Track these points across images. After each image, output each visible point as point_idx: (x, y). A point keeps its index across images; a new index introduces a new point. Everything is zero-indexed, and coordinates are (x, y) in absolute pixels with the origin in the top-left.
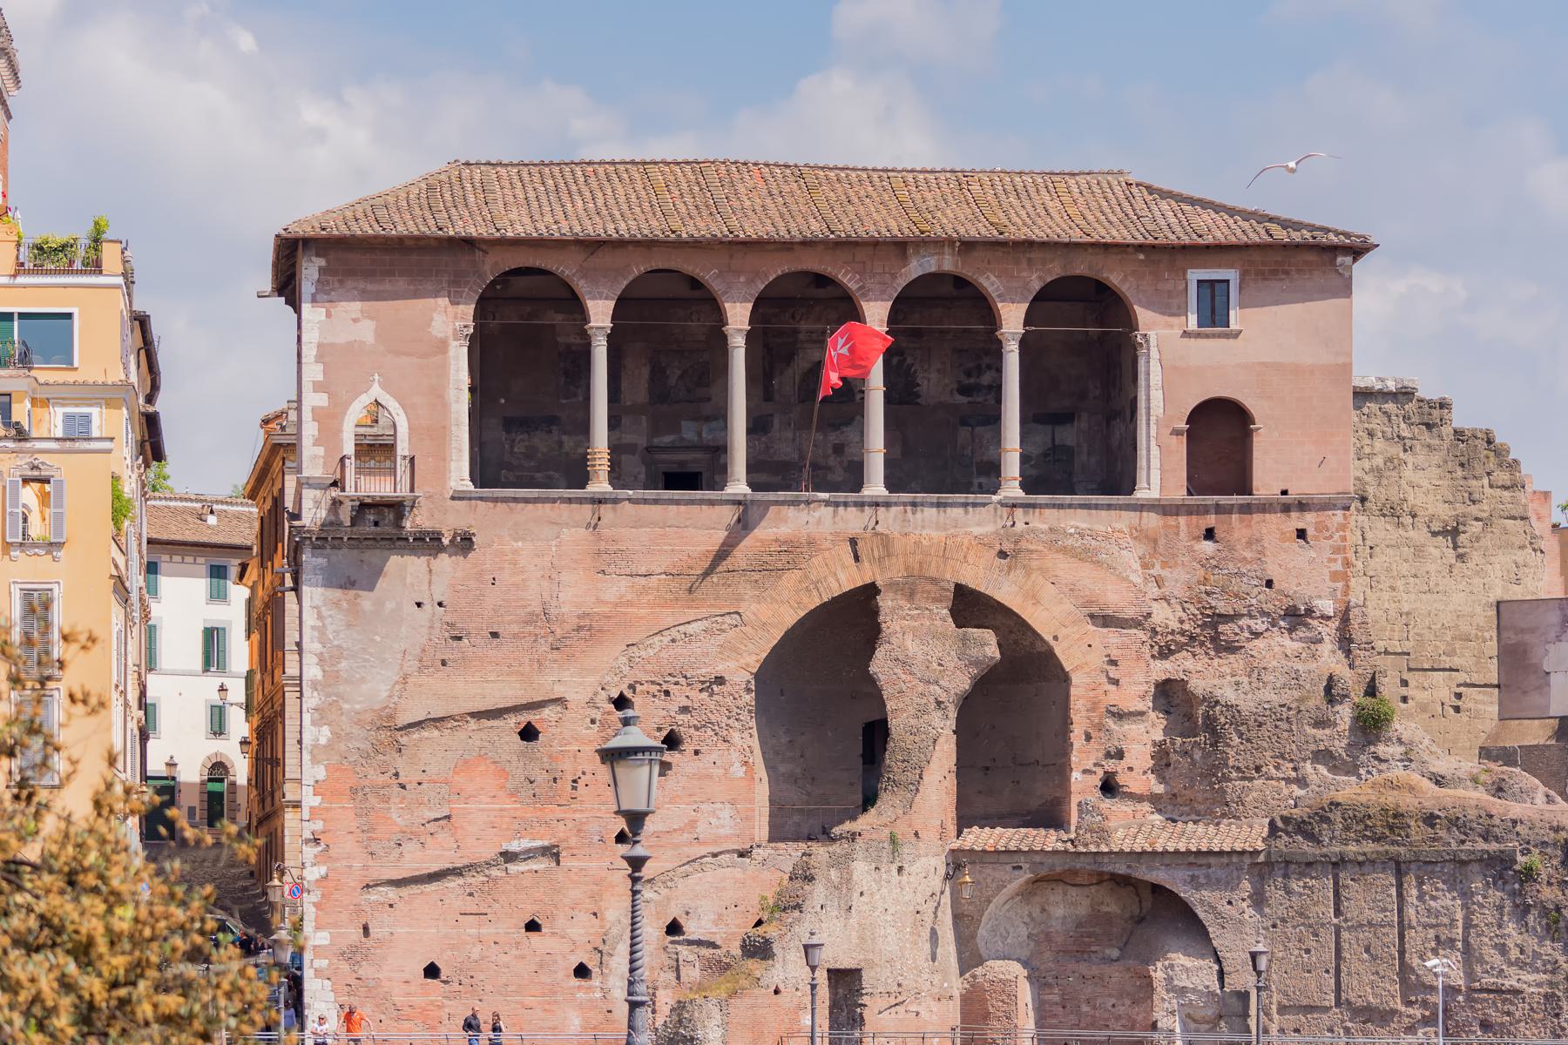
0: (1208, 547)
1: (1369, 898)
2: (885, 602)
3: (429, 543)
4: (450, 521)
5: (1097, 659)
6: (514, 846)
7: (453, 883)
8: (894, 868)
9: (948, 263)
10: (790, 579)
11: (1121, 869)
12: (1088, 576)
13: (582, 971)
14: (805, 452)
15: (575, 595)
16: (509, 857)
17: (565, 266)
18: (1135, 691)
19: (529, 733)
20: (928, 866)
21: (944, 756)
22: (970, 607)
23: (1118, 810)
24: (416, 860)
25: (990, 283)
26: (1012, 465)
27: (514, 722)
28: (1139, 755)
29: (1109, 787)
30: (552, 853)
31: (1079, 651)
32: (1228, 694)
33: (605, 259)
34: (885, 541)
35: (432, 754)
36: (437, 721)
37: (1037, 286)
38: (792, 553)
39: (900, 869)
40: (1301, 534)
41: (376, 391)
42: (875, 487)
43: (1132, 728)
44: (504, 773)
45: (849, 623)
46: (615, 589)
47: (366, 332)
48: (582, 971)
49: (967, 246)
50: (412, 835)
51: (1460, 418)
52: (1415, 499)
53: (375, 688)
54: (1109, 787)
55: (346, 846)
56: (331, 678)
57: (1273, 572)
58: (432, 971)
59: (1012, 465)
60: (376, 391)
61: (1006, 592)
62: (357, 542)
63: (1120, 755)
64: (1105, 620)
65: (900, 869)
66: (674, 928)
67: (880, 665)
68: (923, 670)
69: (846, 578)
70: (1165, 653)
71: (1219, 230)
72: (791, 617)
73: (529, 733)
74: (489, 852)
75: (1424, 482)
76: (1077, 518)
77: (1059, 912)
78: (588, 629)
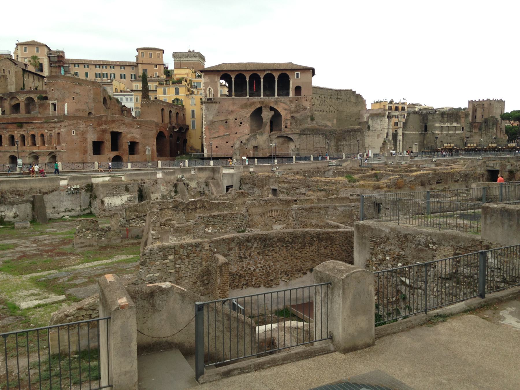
1: (310, 138)
3: (216, 103)
4: (218, 100)
5: (285, 114)
9: (269, 72)
10: (253, 106)
11: (285, 135)
12: (284, 105)
13: (232, 147)
14: (255, 92)
15: (231, 108)
17: (229, 73)
18: (289, 117)
19: (226, 122)
20: (266, 136)
21: (269, 124)
22: (272, 109)
23: (286, 129)
24: (215, 136)
25: (274, 74)
27: (225, 121)
28: (289, 123)
29: (286, 127)
30: (229, 135)
31: (283, 113)
32: (298, 117)
33: (234, 72)
34: (263, 102)
38: (253, 103)
41: (210, 87)
42: (262, 96)
46: (235, 107)
47: (209, 81)
48: (232, 147)
49: (271, 70)
50: (214, 133)
51: (356, 93)
52: (352, 100)
53: (211, 118)
56: (206, 117)
58: (217, 147)
60: (210, 87)
61: (275, 107)
62: (208, 103)
64: (286, 110)
66: (242, 142)
67: (262, 115)
68: (267, 115)
69: (259, 106)
70: (292, 113)
71: (298, 68)
72: (253, 110)
73: (226, 122)
75: (353, 99)
76: (282, 98)
78: (232, 112)
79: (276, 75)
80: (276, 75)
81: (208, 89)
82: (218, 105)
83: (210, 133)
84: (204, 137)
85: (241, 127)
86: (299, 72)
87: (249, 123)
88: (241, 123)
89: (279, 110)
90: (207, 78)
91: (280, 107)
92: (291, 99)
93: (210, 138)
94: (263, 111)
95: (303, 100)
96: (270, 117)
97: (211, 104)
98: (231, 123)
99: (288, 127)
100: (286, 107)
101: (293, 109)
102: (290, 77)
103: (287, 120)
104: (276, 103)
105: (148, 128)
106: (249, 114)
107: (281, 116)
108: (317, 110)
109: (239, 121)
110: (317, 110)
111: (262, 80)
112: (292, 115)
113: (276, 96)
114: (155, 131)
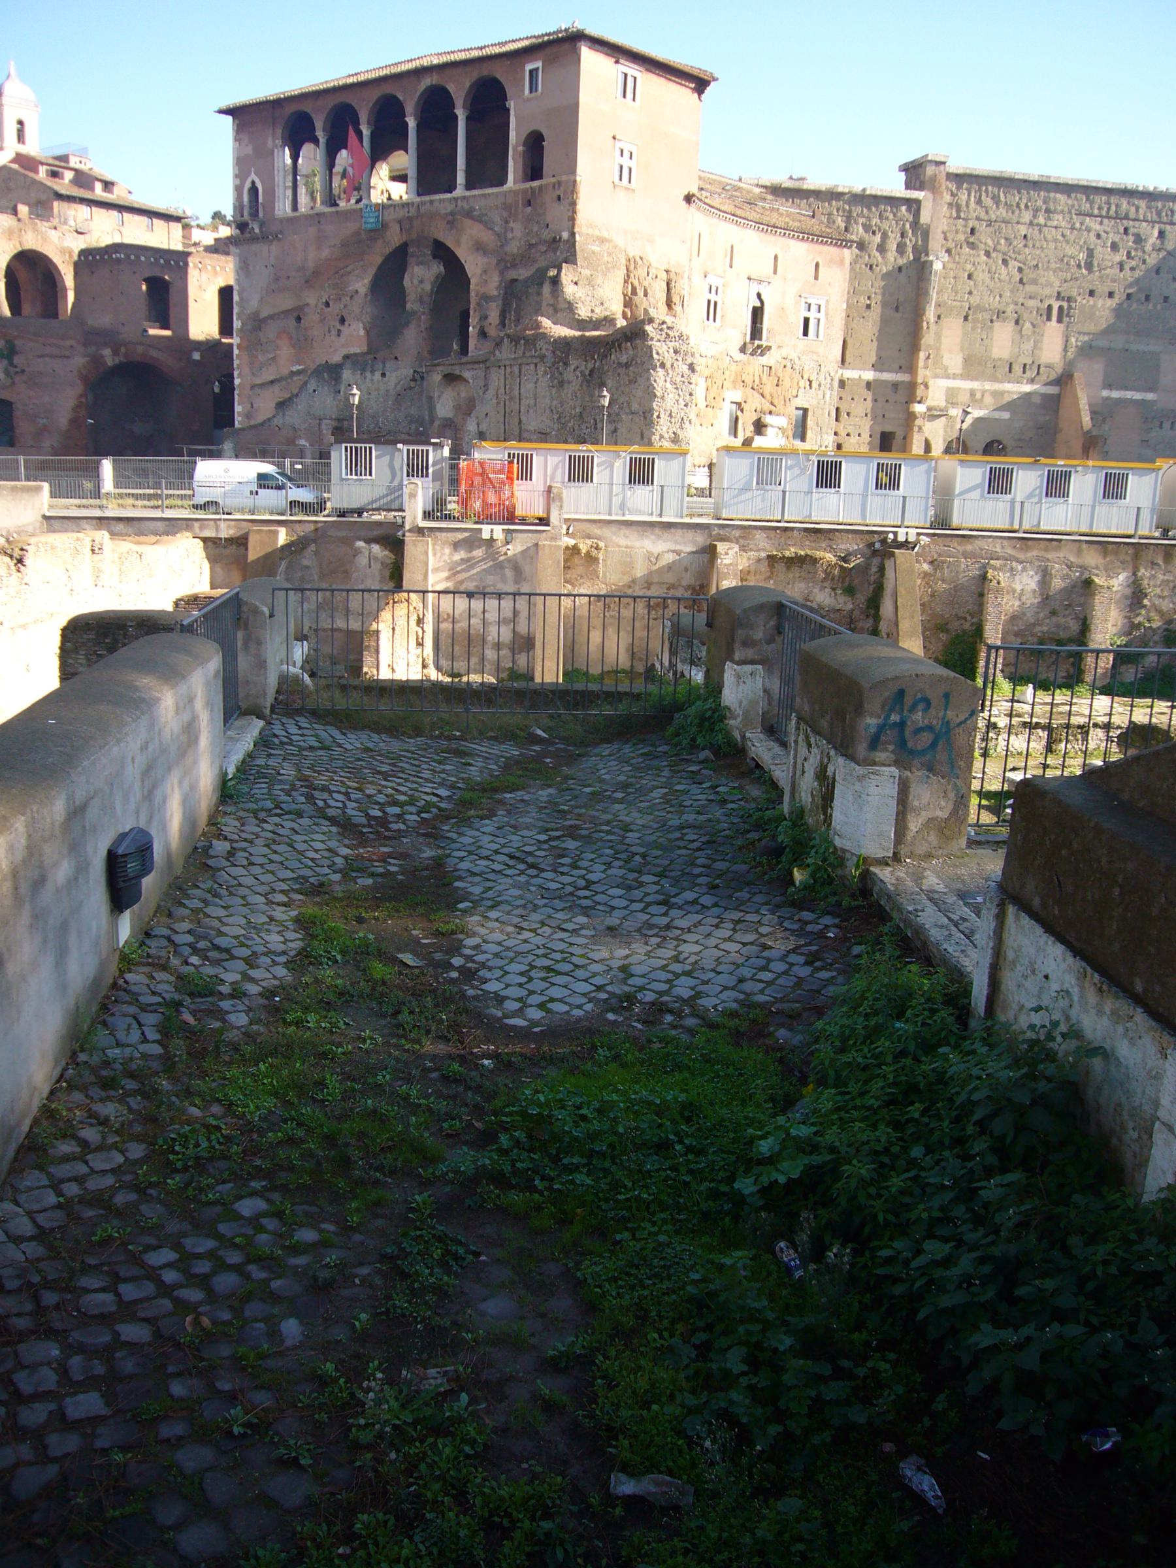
0: (529, 209)
2: (411, 250)
3: (264, 238)
5: (479, 271)
6: (295, 369)
7: (277, 387)
8: (378, 375)
16: (293, 374)
19: (299, 319)
24: (267, 376)
25: (451, 88)
26: (461, 178)
29: (483, 334)
34: (410, 219)
35: (271, 331)
36: (271, 317)
37: (468, 85)
39: (383, 375)
40: (559, 198)
43: (493, 305)
44: (291, 338)
45: (397, 261)
53: (254, 304)
54: (483, 334)
55: (246, 370)
56: (241, 299)
57: (549, 218)
59: (461, 178)
60: (253, 177)
63: (486, 317)
65: (383, 375)
67: (407, 282)
70: (514, 266)
73: (299, 319)
74: (286, 372)
77: (463, 395)
79: (459, 91)
80: (459, 91)
81: (248, 185)
82: (275, 247)
83: (251, 364)
84: (237, 382)
85: (343, 339)
86: (538, 64)
87: (367, 318)
88: (342, 321)
89: (463, 253)
90: (245, 137)
91: (464, 239)
92: (509, 201)
93: (253, 387)
94: (411, 261)
95: (548, 197)
96: (428, 287)
97: (255, 247)
98: (311, 318)
99: (492, 332)
100: (487, 237)
101: (513, 248)
102: (510, 91)
103: (486, 298)
104: (452, 221)
105: (48, 350)
106: (367, 280)
107: (468, 281)
108: (1102, 289)
109: (335, 308)
110: (1102, 289)
111: (412, 123)
112: (512, 274)
113: (459, 191)
114: (79, 361)
